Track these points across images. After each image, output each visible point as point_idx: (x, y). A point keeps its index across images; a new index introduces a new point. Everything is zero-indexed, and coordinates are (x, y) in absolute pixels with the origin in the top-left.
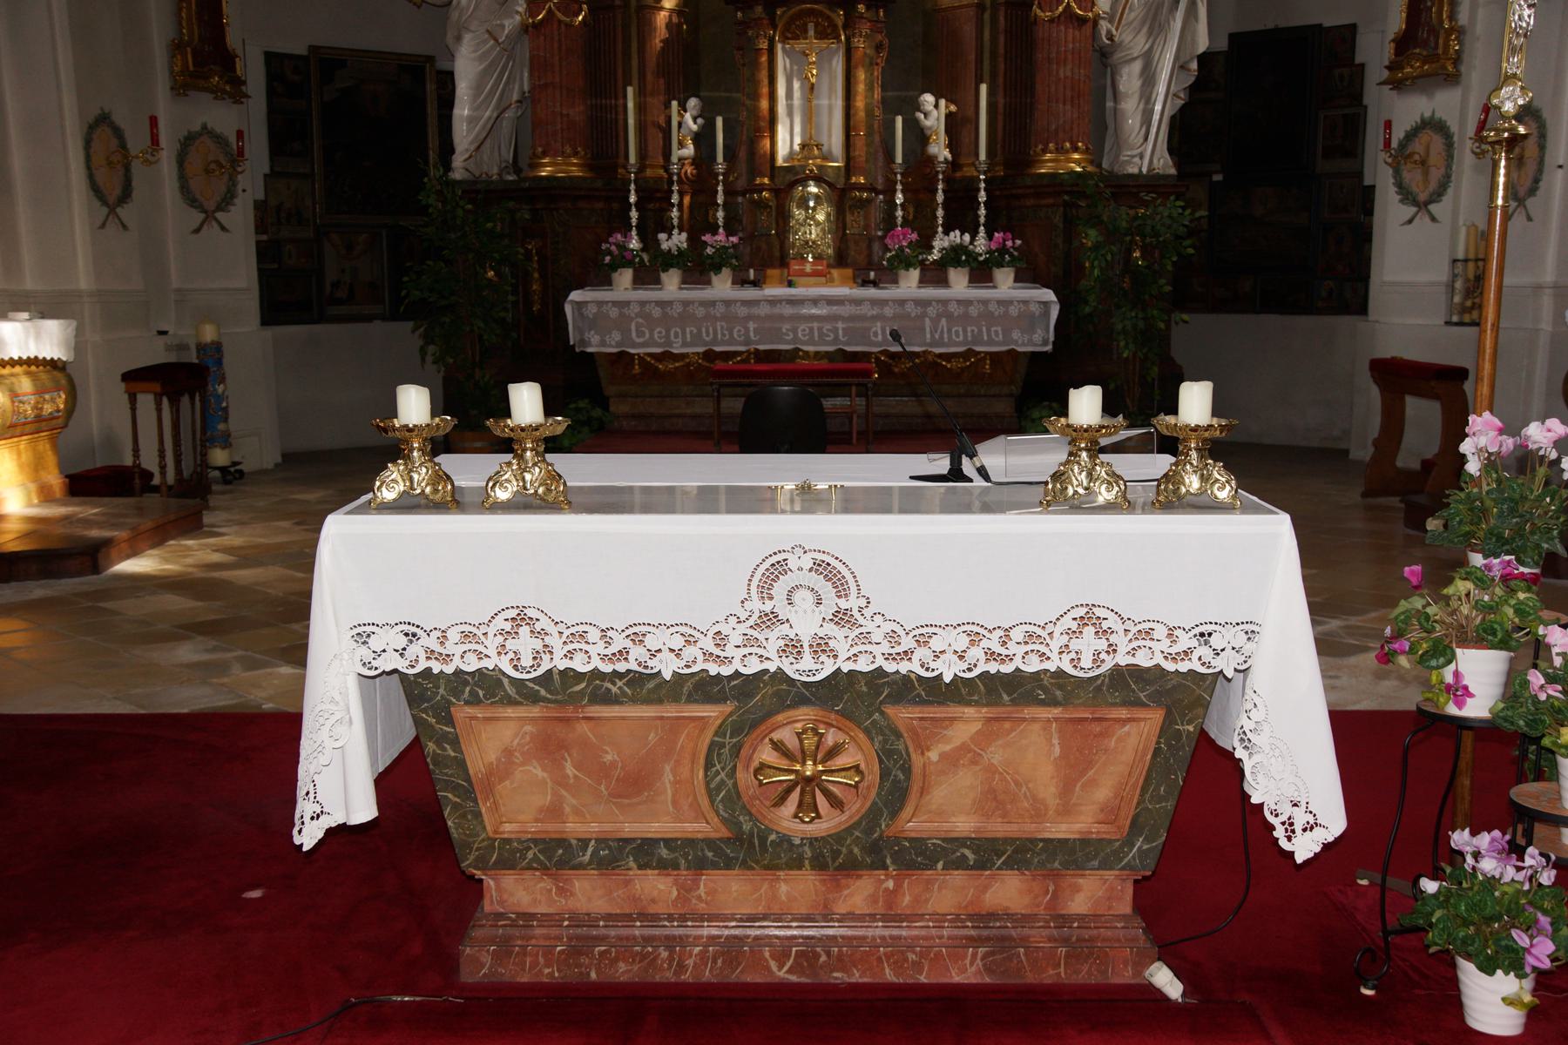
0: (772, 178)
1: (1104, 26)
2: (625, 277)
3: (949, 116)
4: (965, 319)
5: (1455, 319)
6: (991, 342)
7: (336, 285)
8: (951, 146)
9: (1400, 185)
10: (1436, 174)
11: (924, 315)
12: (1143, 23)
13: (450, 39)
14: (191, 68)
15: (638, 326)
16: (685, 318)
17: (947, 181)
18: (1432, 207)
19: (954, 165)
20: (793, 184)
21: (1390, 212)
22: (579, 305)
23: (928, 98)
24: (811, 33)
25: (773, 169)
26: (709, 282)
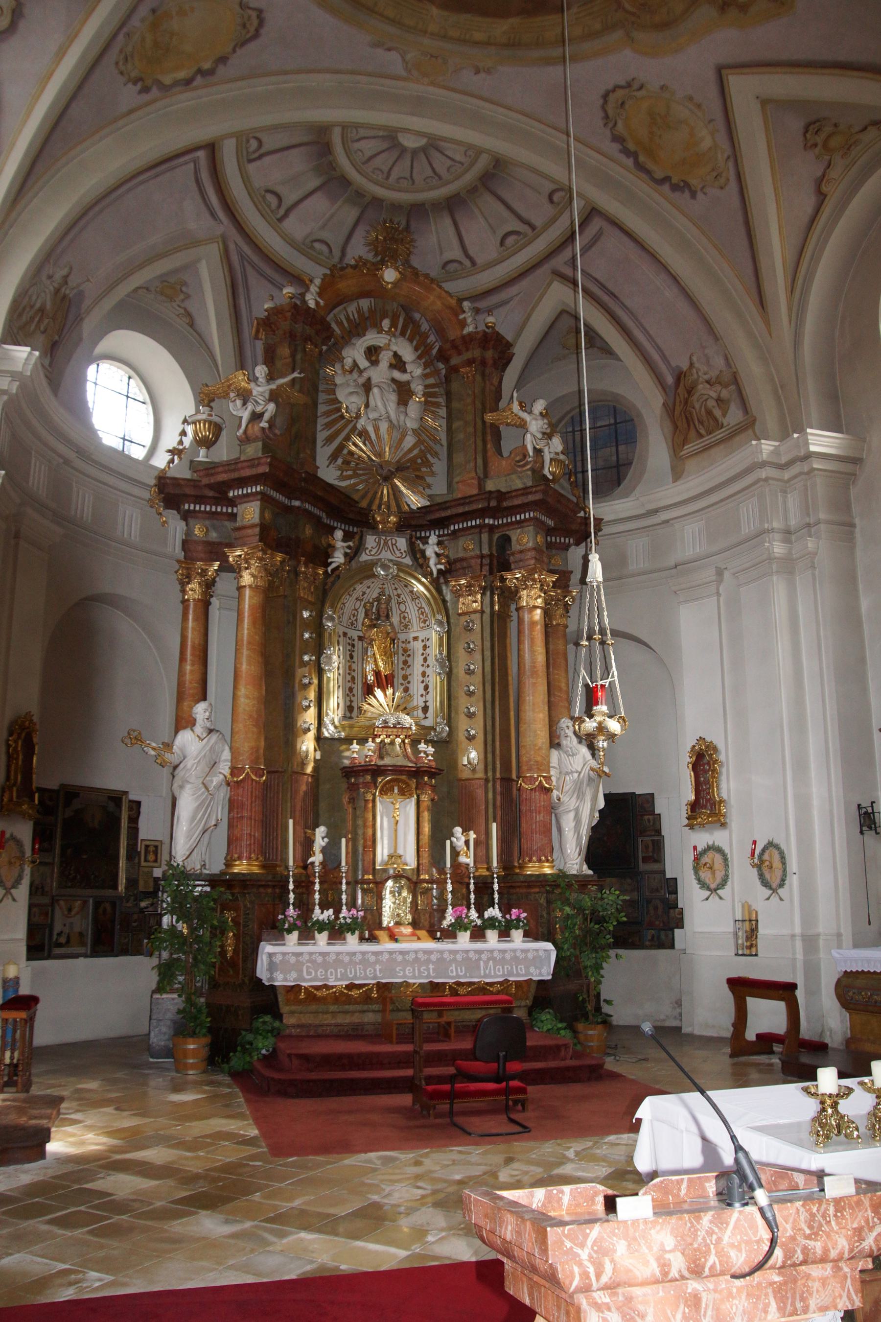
0: (374, 875)
1: (555, 793)
2: (295, 934)
4: (503, 962)
5: (740, 952)
6: (518, 975)
7: (59, 934)
9: (699, 880)
11: (480, 959)
12: (574, 792)
14: (15, 799)
15: (308, 967)
16: (338, 962)
18: (718, 891)
22: (270, 955)
24: (396, 791)
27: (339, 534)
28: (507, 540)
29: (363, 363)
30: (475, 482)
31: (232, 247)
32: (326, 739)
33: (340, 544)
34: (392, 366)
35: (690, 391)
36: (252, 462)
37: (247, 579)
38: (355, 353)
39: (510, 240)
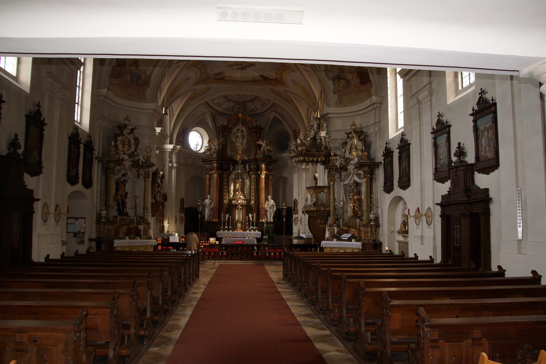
1: (266, 208)
2: (222, 230)
3: (252, 216)
8: (252, 219)
9: (294, 223)
10: (297, 222)
13: (205, 207)
17: (252, 222)
19: (252, 220)
20: (237, 222)
21: (294, 225)
22: (218, 233)
23: (250, 214)
25: (235, 221)
26: (229, 231)
27: (231, 165)
28: (259, 166)
29: (236, 132)
30: (254, 155)
31: (212, 112)
32: (230, 200)
33: (231, 167)
34: (241, 132)
35: (296, 133)
36: (215, 158)
37: (215, 176)
38: (235, 130)
39: (263, 105)
